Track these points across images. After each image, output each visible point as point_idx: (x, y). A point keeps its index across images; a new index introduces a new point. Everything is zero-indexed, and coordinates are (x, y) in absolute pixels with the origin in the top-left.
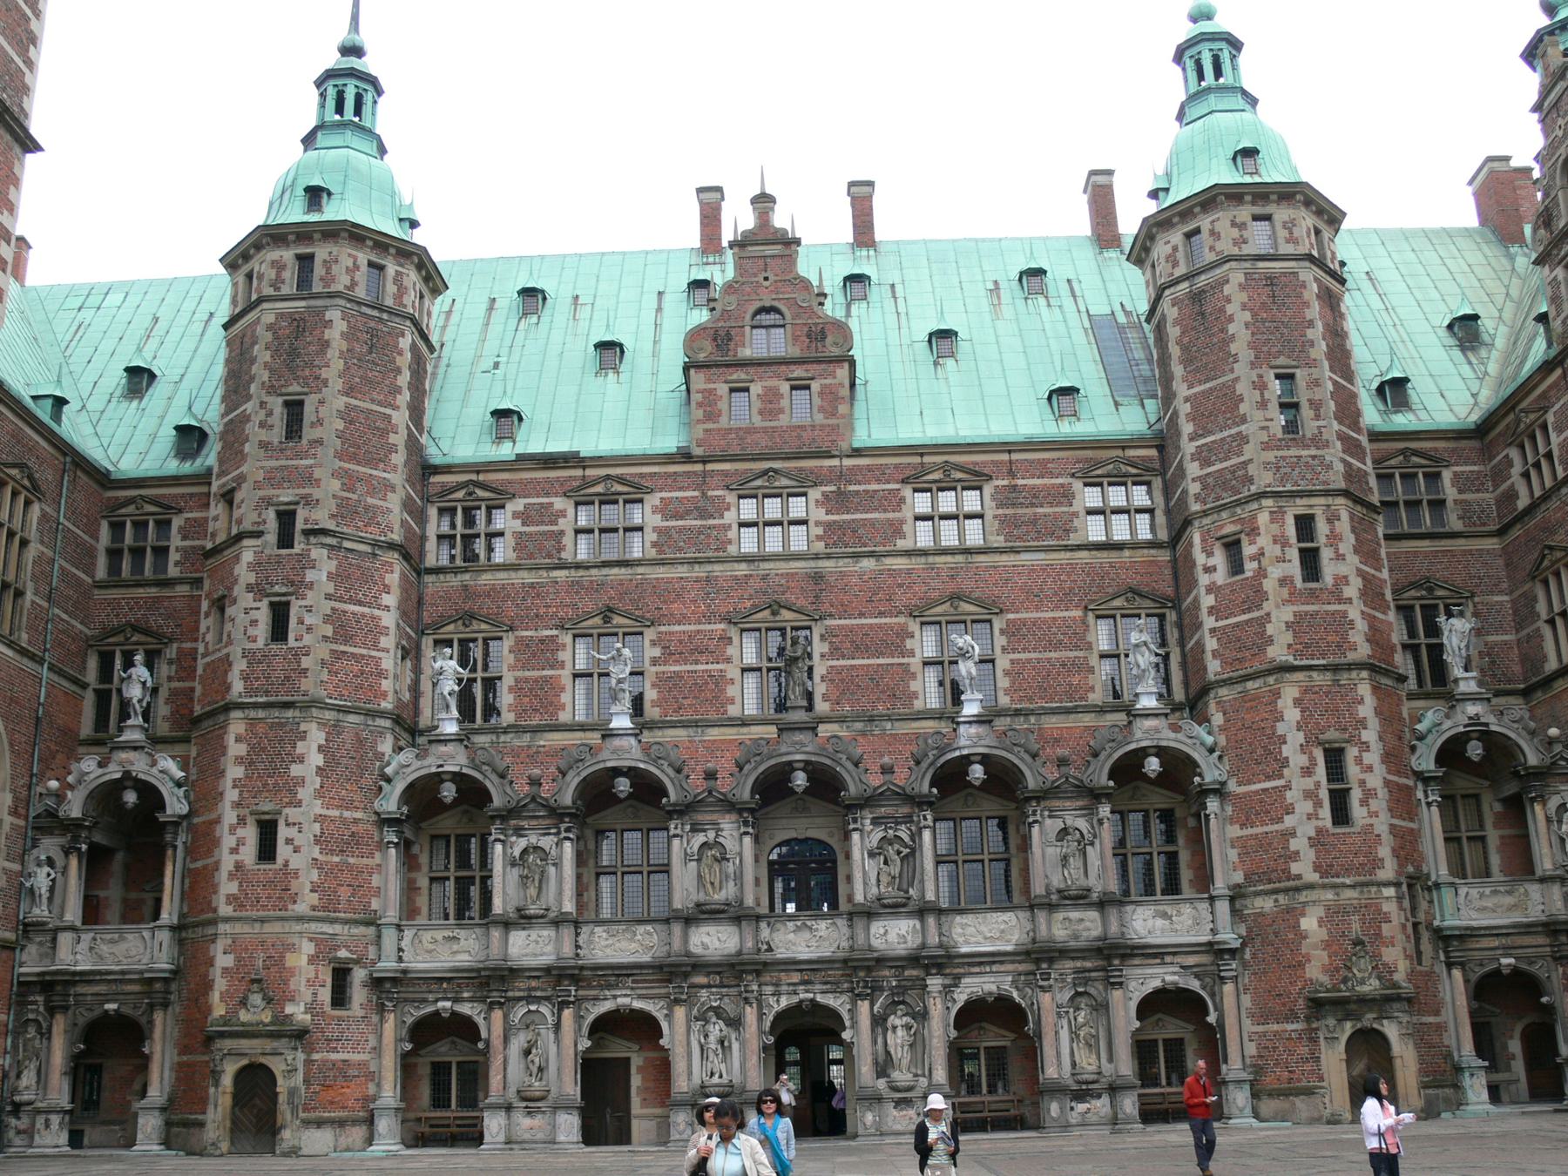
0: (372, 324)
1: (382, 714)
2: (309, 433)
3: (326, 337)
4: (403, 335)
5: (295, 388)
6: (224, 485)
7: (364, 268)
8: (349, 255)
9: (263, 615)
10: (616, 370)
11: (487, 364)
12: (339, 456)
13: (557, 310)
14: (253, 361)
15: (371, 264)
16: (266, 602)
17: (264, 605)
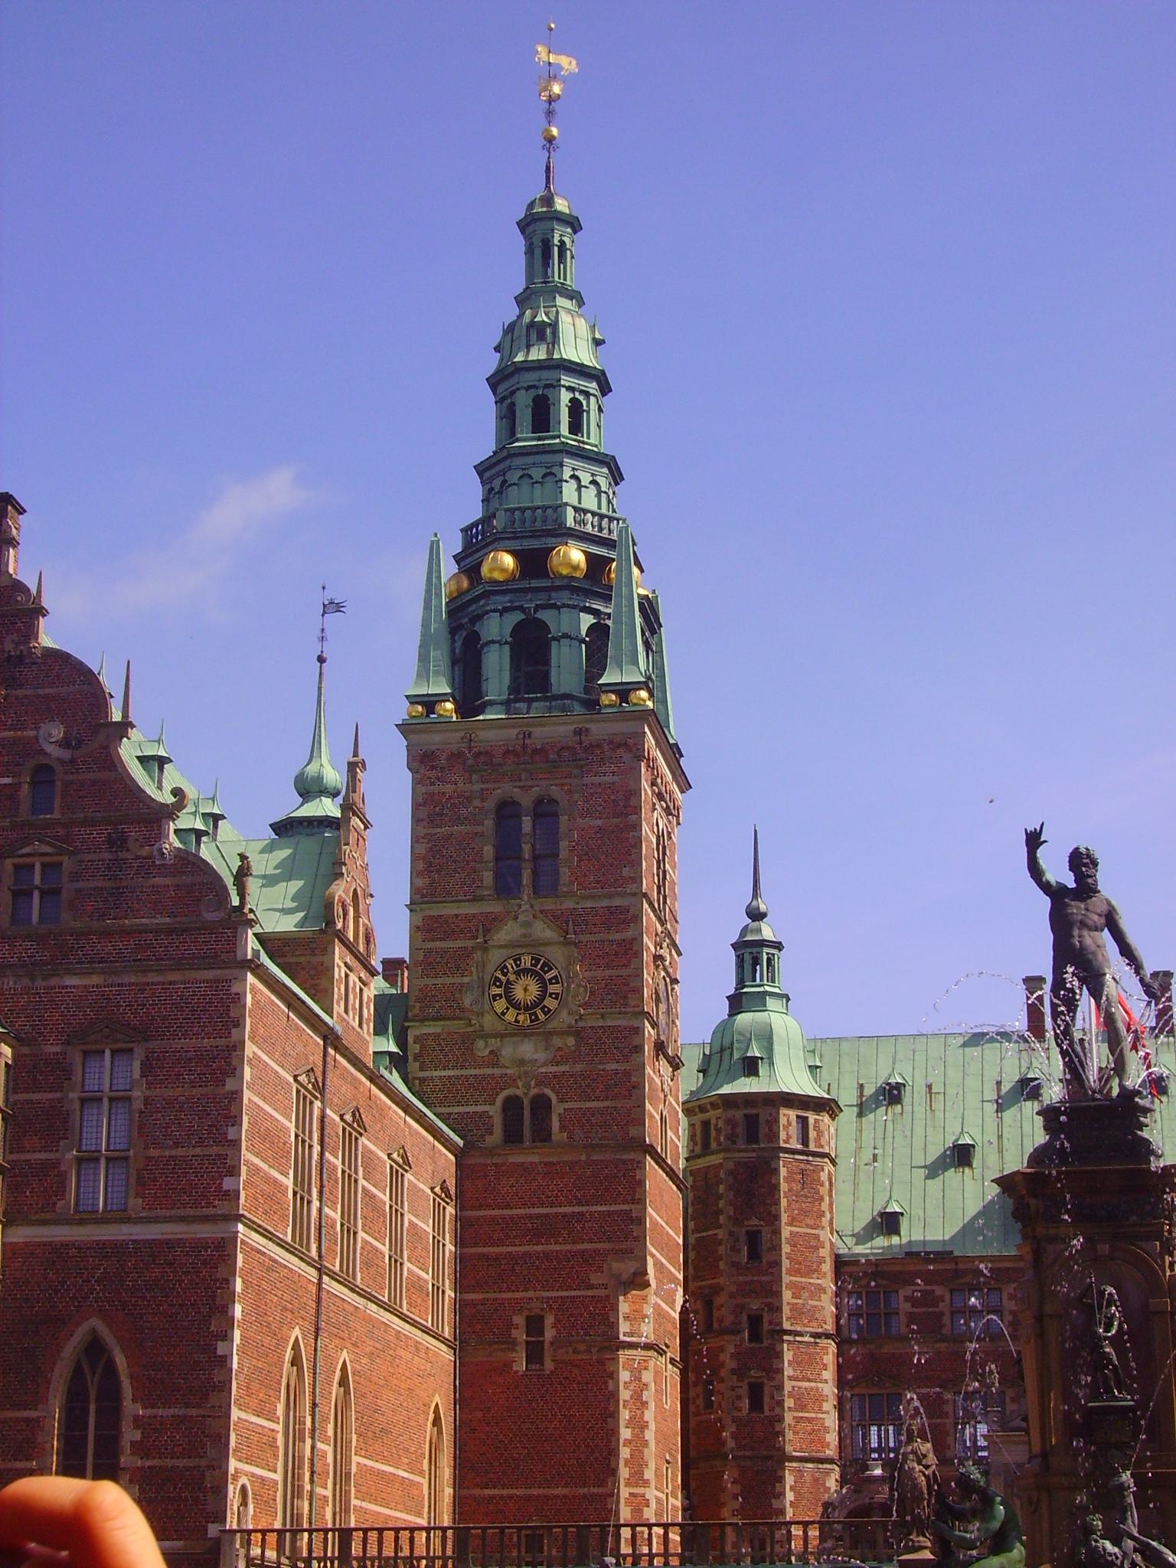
0: (802, 1166)
1: (830, 1461)
2: (767, 1257)
3: (773, 1182)
4: (823, 1170)
5: (755, 1222)
6: (701, 1288)
7: (794, 1123)
8: (784, 1115)
9: (744, 1391)
10: (969, 1165)
11: (867, 1156)
12: (789, 1273)
13: (914, 1097)
14: (720, 1197)
15: (798, 1116)
16: (746, 1381)
17: (745, 1385)
